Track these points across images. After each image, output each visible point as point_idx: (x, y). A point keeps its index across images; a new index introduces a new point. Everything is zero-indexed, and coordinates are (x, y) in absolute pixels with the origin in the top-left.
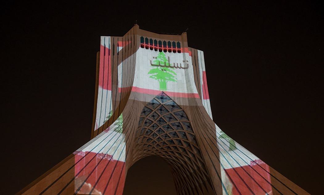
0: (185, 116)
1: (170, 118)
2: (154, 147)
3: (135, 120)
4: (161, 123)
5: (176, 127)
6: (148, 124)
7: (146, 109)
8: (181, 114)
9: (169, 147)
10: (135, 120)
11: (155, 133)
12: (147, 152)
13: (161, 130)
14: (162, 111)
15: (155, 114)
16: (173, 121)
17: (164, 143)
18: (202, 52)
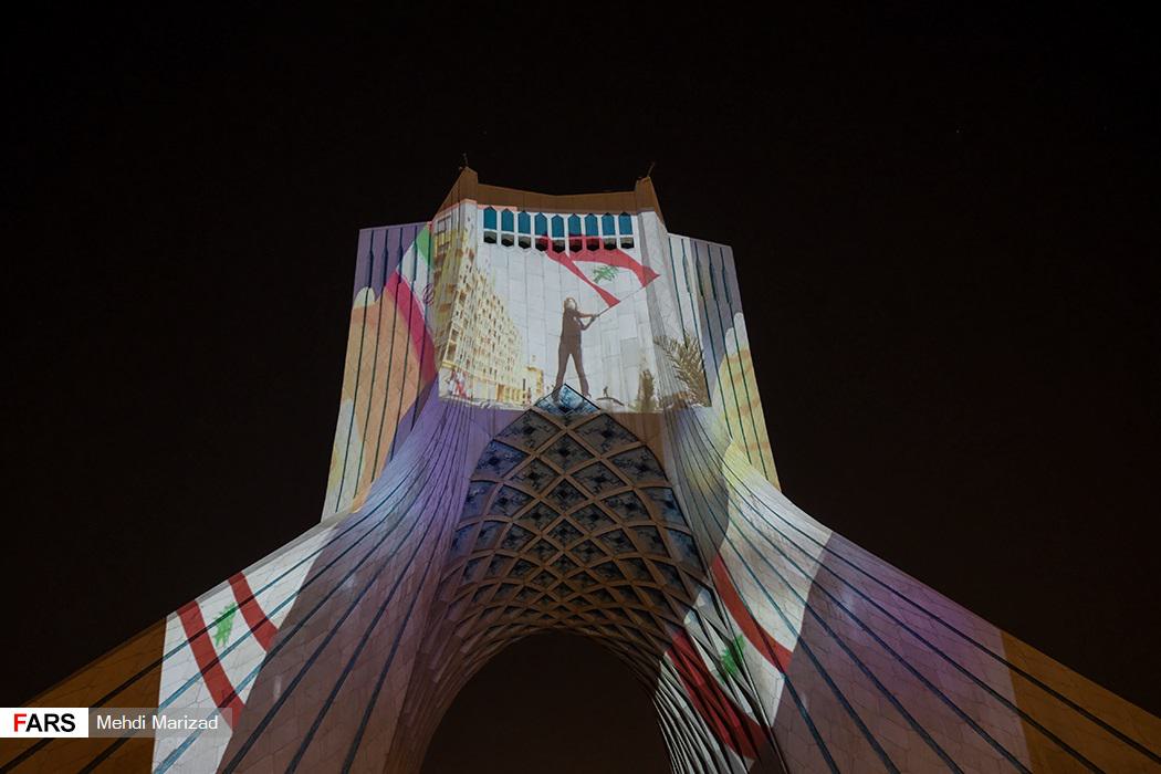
0: (652, 465)
1: (600, 480)
2: (546, 597)
3: (446, 487)
4: (567, 500)
5: (622, 512)
6: (511, 508)
7: (501, 452)
8: (640, 461)
9: (605, 593)
10: (446, 487)
11: (543, 540)
12: (524, 614)
13: (569, 529)
14: (569, 457)
15: (539, 470)
16: (609, 491)
17: (586, 577)
18: (728, 250)
